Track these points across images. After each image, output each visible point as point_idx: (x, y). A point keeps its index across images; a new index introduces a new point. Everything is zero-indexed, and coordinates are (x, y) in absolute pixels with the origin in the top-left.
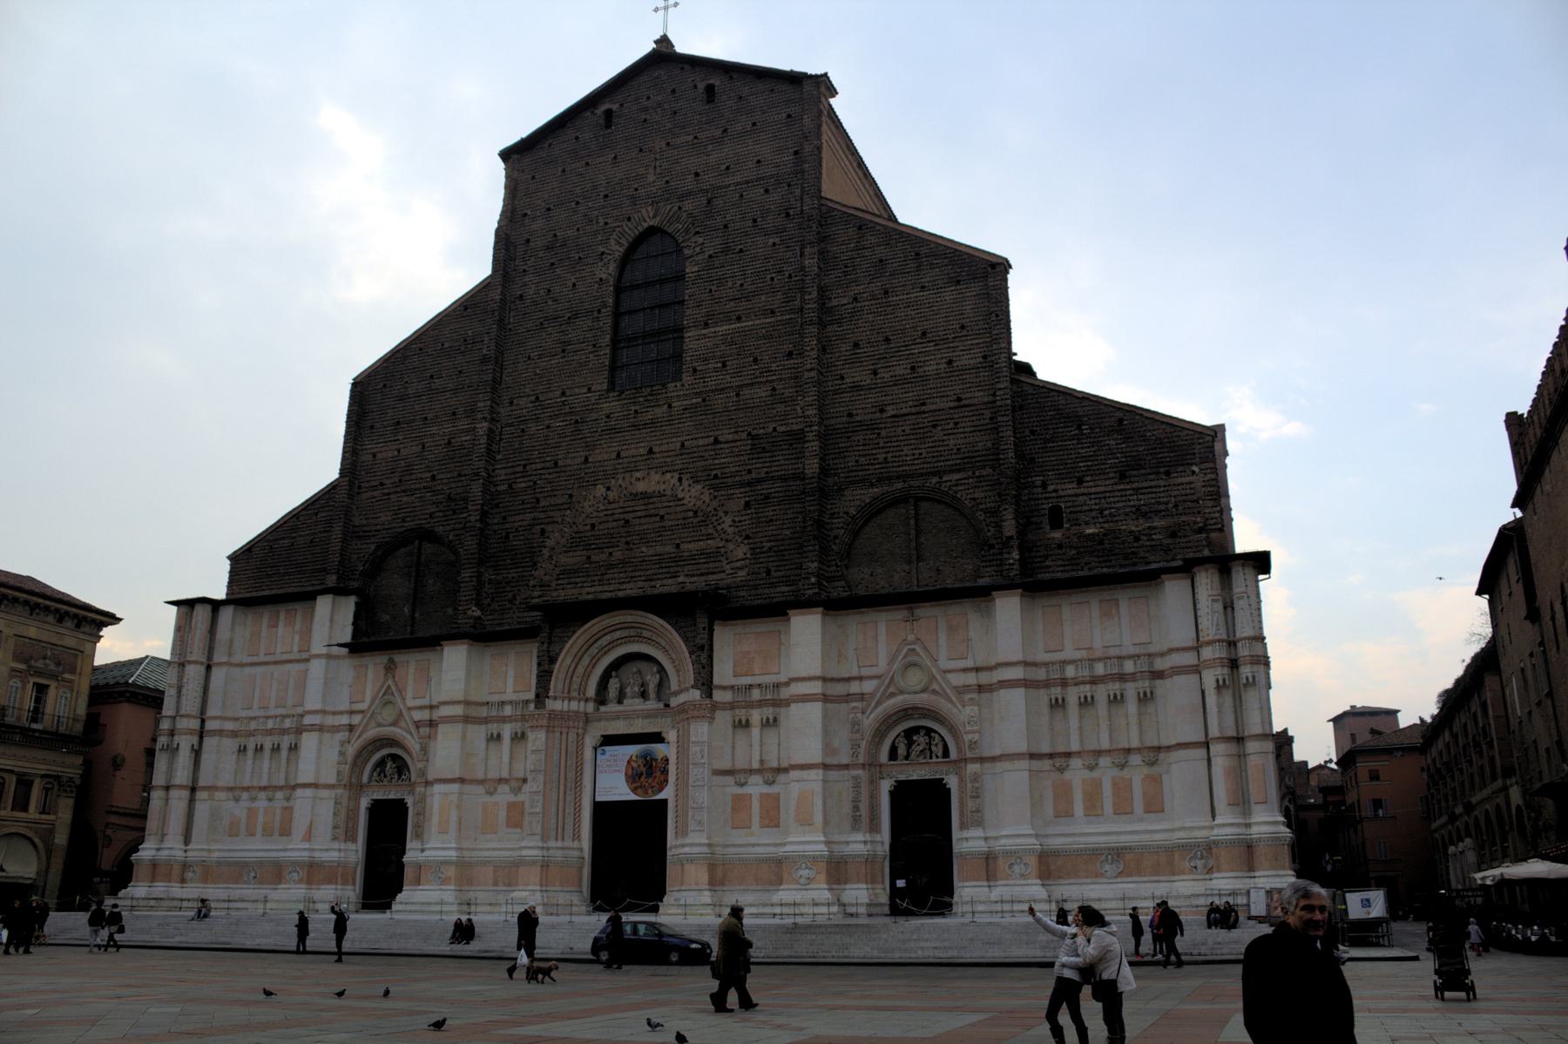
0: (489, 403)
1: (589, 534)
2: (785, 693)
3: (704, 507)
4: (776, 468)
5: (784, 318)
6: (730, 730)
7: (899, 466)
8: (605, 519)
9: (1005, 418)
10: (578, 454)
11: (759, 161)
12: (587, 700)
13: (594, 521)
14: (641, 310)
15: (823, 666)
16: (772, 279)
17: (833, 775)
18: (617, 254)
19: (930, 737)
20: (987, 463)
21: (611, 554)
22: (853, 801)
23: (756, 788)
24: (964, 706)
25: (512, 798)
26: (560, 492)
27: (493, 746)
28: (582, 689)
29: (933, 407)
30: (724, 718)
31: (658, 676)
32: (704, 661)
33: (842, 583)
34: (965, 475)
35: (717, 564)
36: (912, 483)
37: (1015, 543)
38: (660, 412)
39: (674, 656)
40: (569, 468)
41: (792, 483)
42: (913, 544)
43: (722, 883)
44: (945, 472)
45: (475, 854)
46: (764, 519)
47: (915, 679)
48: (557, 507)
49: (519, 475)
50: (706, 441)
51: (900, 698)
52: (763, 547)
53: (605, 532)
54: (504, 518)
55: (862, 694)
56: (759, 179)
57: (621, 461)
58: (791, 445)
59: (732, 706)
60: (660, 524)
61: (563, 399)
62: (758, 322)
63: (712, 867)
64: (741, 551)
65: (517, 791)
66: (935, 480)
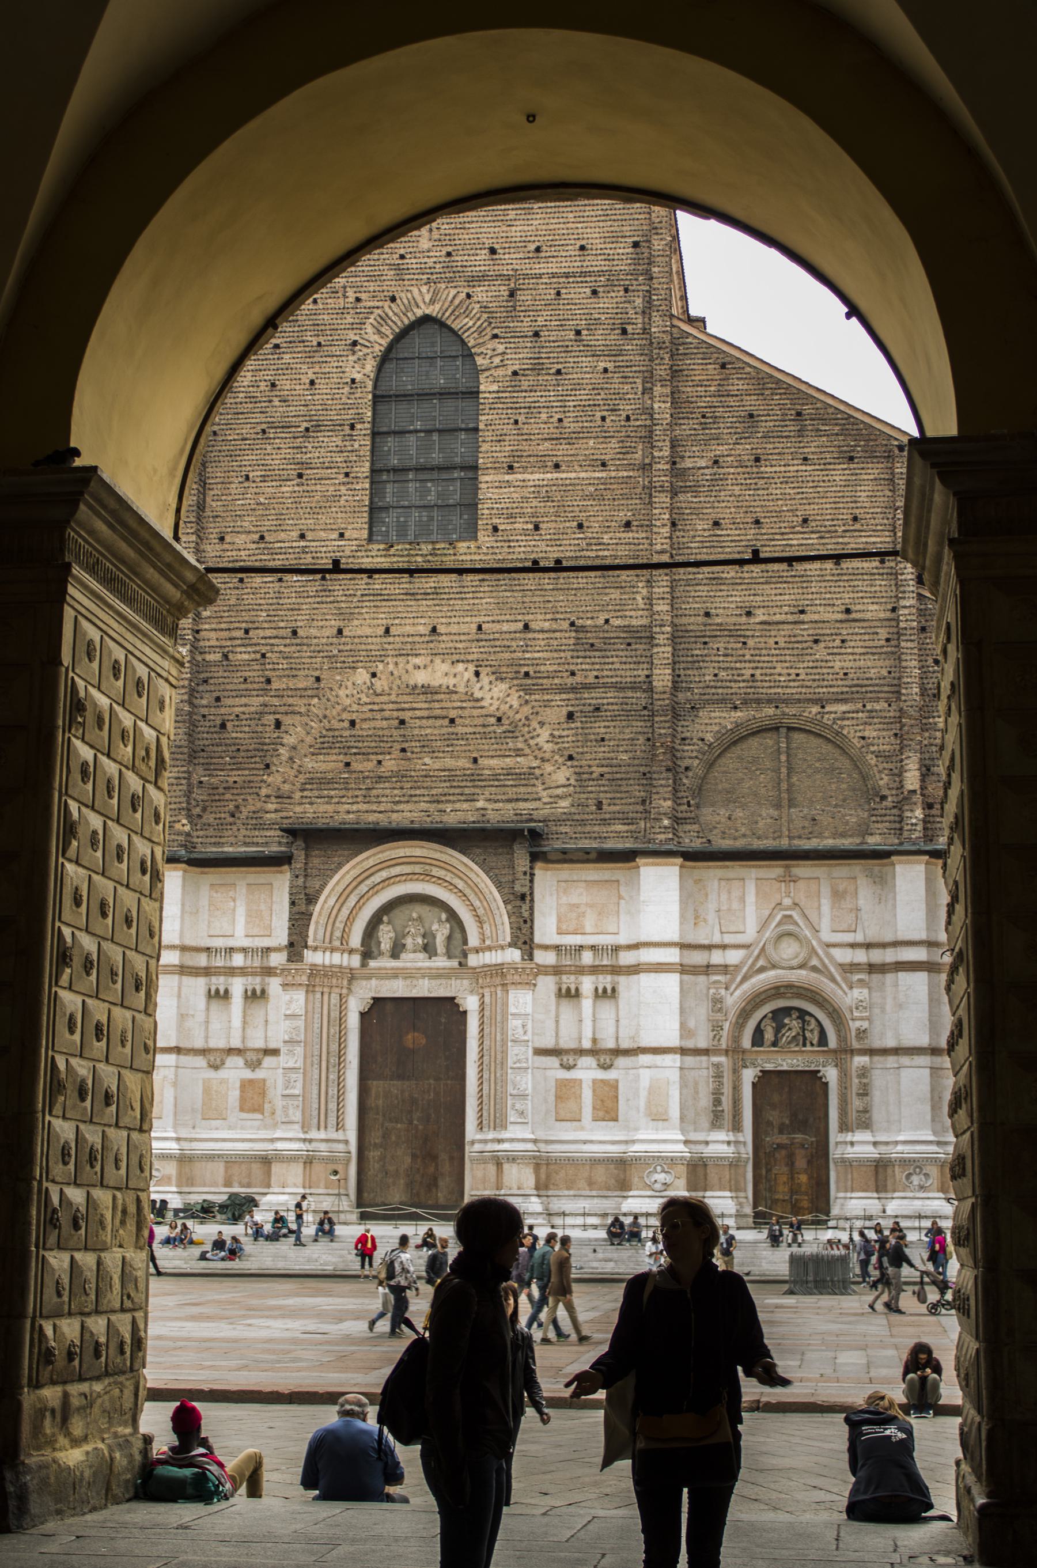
0: (194, 538)
1: (347, 733)
2: (626, 958)
3: (511, 713)
4: (609, 673)
5: (621, 474)
6: (553, 998)
7: (770, 687)
8: (369, 715)
9: (909, 644)
10: (327, 623)
11: (582, 248)
12: (351, 952)
13: (354, 716)
15: (681, 930)
16: (603, 419)
17: (690, 1060)
18: (377, 348)
19: (804, 1021)
20: (880, 695)
21: (380, 762)
22: (713, 1094)
23: (587, 1072)
25: (248, 1074)
26: (302, 673)
27: (215, 1005)
28: (344, 938)
29: (816, 617)
30: (547, 984)
31: (448, 926)
32: (526, 914)
33: (696, 827)
34: (853, 708)
35: (530, 789)
36: (787, 710)
37: (918, 798)
39: (477, 904)
40: (316, 641)
41: (630, 694)
42: (784, 786)
43: (547, 1188)
45: (195, 1145)
46: (592, 737)
47: (789, 951)
48: (298, 693)
49: (239, 642)
50: (514, 626)
51: (772, 974)
52: (591, 773)
53: (370, 733)
54: (218, 699)
55: (726, 966)
56: (584, 274)
57: (391, 639)
58: (629, 644)
59: (557, 971)
60: (450, 730)
61: (302, 544)
62: (583, 475)
63: (537, 1167)
64: (562, 775)
65: (254, 1065)
66: (815, 709)
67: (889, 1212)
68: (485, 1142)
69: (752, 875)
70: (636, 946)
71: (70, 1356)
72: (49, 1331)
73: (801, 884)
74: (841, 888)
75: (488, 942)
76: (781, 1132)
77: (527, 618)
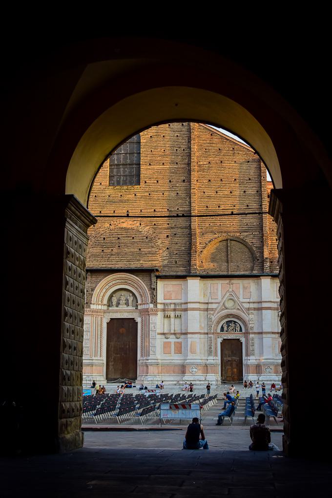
1: (103, 241)
8: (109, 236)
14: (120, 154)
16: (177, 150)
23: (172, 339)
24: (249, 315)
38: (132, 196)
42: (229, 257)
44: (242, 232)
47: (229, 304)
51: (226, 311)
59: (164, 310)
60: (133, 241)
64: (165, 254)
66: (238, 234)
67: (260, 380)
68: (143, 360)
69: (219, 284)
70: (187, 303)
71: (68, 411)
72: (64, 405)
73: (234, 285)
74: (246, 286)
75: (144, 302)
76: (229, 357)
77: (155, 208)
